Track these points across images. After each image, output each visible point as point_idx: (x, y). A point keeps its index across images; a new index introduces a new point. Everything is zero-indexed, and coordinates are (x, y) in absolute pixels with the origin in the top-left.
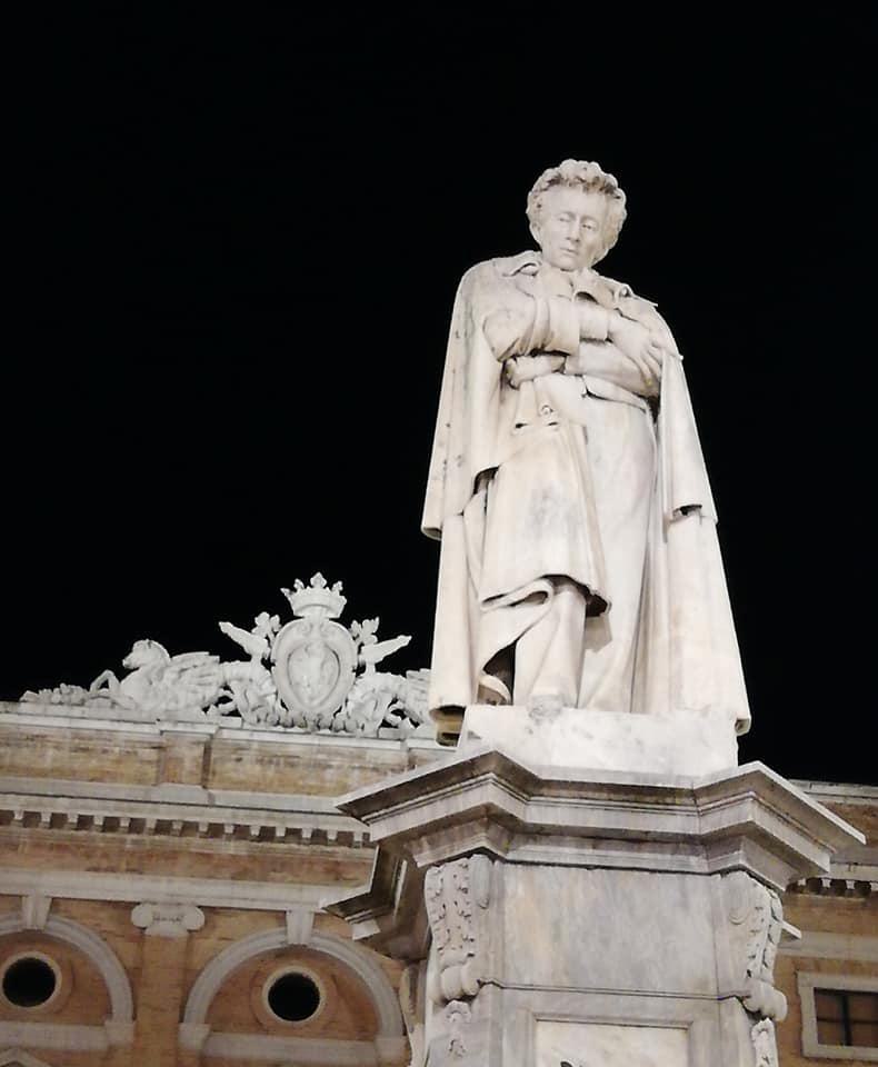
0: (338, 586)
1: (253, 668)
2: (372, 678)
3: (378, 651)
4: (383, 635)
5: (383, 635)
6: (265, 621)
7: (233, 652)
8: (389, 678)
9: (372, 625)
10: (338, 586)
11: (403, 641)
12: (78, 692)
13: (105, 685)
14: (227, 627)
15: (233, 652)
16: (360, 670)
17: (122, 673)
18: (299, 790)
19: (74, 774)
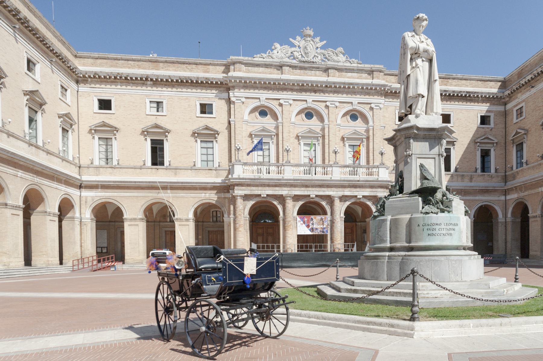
0: (312, 29)
1: (297, 49)
2: (319, 51)
3: (320, 45)
4: (321, 41)
6: (298, 38)
7: (292, 45)
9: (318, 38)
10: (312, 29)
12: (264, 55)
13: (269, 53)
14: (291, 39)
15: (292, 45)
17: (272, 50)
18: (308, 76)
19: (266, 73)
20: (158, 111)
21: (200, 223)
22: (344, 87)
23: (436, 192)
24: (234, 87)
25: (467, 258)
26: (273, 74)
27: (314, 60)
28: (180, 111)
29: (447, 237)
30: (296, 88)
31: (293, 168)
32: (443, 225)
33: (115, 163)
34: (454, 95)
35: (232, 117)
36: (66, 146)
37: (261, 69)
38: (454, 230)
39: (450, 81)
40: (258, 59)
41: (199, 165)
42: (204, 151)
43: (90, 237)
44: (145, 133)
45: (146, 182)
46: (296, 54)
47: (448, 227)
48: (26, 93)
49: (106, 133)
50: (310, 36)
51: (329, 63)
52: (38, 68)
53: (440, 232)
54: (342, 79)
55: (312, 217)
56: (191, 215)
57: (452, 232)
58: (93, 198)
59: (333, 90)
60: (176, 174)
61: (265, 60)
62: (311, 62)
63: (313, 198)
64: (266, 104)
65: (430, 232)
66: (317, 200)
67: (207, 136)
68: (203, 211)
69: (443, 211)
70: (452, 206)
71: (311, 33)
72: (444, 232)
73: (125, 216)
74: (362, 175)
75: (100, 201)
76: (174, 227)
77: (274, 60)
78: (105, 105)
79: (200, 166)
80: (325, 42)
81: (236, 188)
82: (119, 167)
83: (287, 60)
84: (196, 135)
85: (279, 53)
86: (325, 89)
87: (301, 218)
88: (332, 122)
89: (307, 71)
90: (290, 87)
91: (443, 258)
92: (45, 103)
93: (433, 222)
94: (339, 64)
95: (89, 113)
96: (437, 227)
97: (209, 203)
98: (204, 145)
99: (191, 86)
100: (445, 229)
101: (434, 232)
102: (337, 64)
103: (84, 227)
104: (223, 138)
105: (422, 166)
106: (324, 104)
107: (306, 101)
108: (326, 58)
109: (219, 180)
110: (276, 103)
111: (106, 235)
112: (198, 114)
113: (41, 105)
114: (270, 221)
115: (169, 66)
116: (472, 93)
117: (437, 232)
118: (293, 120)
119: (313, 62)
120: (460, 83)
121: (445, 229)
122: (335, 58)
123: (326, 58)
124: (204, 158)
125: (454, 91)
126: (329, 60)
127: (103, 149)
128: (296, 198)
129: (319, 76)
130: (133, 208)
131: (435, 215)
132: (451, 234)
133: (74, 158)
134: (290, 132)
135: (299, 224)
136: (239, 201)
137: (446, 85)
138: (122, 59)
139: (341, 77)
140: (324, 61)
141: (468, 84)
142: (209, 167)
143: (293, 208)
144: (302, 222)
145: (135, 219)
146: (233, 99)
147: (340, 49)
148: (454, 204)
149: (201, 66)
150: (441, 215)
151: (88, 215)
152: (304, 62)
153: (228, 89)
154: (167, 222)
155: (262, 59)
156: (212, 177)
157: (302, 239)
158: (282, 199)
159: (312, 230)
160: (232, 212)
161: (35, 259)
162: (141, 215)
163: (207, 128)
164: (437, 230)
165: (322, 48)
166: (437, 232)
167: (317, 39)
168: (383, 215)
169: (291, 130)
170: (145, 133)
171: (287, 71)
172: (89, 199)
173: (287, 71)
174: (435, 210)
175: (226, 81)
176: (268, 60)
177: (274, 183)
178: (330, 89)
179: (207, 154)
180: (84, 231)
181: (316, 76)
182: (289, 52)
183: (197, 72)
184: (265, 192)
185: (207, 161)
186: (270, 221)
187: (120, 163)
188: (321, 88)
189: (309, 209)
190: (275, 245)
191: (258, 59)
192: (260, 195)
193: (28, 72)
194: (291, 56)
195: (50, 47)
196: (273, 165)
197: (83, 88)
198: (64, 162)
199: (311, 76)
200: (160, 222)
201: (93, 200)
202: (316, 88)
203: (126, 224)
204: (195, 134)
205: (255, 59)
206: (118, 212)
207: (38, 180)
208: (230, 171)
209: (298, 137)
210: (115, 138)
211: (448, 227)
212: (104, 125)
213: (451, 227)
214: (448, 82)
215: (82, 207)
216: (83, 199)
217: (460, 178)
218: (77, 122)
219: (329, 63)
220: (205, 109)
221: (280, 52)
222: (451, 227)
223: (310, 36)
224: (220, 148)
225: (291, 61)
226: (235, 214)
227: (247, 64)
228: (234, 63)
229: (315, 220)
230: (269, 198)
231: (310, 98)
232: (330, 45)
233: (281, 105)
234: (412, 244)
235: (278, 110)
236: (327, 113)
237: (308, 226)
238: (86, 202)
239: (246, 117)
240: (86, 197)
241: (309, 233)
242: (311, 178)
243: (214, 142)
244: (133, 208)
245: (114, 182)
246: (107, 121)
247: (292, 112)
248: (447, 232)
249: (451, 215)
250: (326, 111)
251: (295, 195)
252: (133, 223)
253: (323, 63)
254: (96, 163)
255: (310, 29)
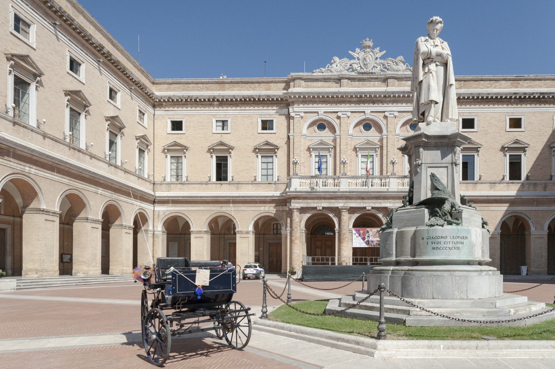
0: (371, 40)
1: (356, 61)
2: (378, 61)
3: (379, 55)
4: (381, 51)
5: (380, 51)
6: (358, 50)
7: (351, 58)
8: (382, 61)
9: (378, 49)
10: (371, 40)
11: (385, 52)
12: (323, 70)
13: (328, 67)
14: (350, 52)
15: (351, 58)
16: (377, 58)
17: (331, 64)
18: (366, 87)
19: (324, 87)
20: (223, 129)
21: (261, 236)
22: (404, 96)
23: (444, 203)
24: (293, 103)
25: (476, 274)
26: (332, 87)
27: (373, 71)
28: (244, 128)
29: (454, 251)
30: (354, 100)
31: (349, 180)
32: (449, 237)
33: (184, 179)
34: (525, 97)
35: (291, 131)
36: (142, 165)
37: (320, 84)
38: (462, 243)
39: (521, 82)
40: (317, 74)
41: (259, 179)
42: (265, 166)
43: (161, 248)
44: (211, 150)
45: (211, 197)
46: (355, 66)
47: (455, 241)
48: (108, 119)
49: (176, 152)
50: (369, 47)
51: (389, 72)
52: (119, 96)
53: (445, 246)
54: (402, 88)
55: (368, 229)
56: (251, 228)
57: (460, 246)
58: (164, 212)
59: (392, 99)
60: (238, 188)
61: (324, 74)
62: (370, 73)
63: (369, 210)
64: (324, 118)
65: (435, 246)
66: (373, 212)
67: (267, 151)
68: (264, 224)
69: (450, 223)
70: (461, 218)
71: (371, 44)
72: (451, 245)
73: (192, 229)
74: (376, 186)
75: (170, 215)
76: (235, 240)
77: (333, 74)
78: (177, 126)
79: (260, 180)
80: (385, 52)
81: (293, 201)
82: (188, 183)
83: (345, 72)
84: (257, 150)
85: (338, 66)
86: (384, 99)
87: (356, 231)
88: (391, 132)
89: (366, 82)
90: (348, 99)
91: (446, 274)
92: (124, 127)
93: (437, 235)
94: (399, 73)
95: (163, 134)
96: (442, 240)
97: (269, 216)
98: (265, 160)
99: (253, 104)
100: (451, 243)
101: (439, 246)
102: (396, 73)
103: (156, 239)
104: (282, 153)
105: (433, 176)
106: (383, 114)
107: (364, 112)
108: (386, 68)
109: (278, 194)
110: (334, 115)
111: (177, 246)
112: (260, 130)
113: (120, 129)
114: (328, 234)
115: (234, 87)
116: (547, 93)
117: (442, 245)
118: (351, 132)
119: (372, 73)
120: (533, 84)
121: (451, 243)
122: (395, 67)
123: (386, 68)
124: (265, 172)
125: (525, 94)
126: (388, 70)
127: (174, 167)
128: (352, 210)
129: (377, 87)
130: (199, 221)
131: (440, 227)
132: (458, 248)
133: (149, 176)
134: (347, 144)
135: (354, 237)
136: (296, 214)
137: (516, 87)
138: (193, 83)
139: (400, 86)
140: (384, 71)
141: (542, 85)
142: (269, 181)
143: (348, 220)
144: (357, 235)
145: (200, 232)
146: (292, 114)
147: (401, 58)
148: (464, 215)
149: (263, 84)
150: (447, 227)
151: (160, 227)
152: (362, 73)
153: (288, 105)
154: (231, 234)
155: (321, 74)
156: (271, 191)
157: (356, 251)
158: (337, 211)
159: (368, 243)
160: (289, 225)
161: (113, 268)
162: (206, 228)
163: (268, 144)
164: (442, 243)
165: (382, 58)
166: (442, 245)
167: (377, 50)
168: (391, 228)
169: (349, 142)
170: (211, 150)
171: (345, 83)
172: (161, 213)
173: (345, 83)
174: (441, 221)
175: (286, 97)
176: (327, 74)
177: (330, 196)
178: (388, 99)
179: (267, 169)
180: (156, 243)
181: (374, 86)
182: (348, 65)
183: (260, 90)
184: (321, 205)
185: (267, 175)
186: (328, 234)
187: (189, 179)
188: (380, 99)
189: (365, 221)
190: (330, 258)
191: (317, 74)
192: (316, 208)
193: (110, 100)
194: (349, 69)
195: (130, 76)
196: (331, 178)
197: (159, 112)
198: (140, 179)
199: (370, 87)
200: (224, 234)
201: (164, 214)
202: (375, 99)
203: (192, 236)
204: (257, 150)
205: (314, 74)
206: (187, 226)
207: (115, 196)
208: (288, 185)
209: (355, 149)
210: (185, 156)
211: (455, 241)
212: (176, 144)
213: (458, 240)
214: (519, 83)
215: (155, 220)
216: (156, 213)
217: (531, 187)
218: (152, 143)
219: (389, 72)
220: (267, 125)
221: (339, 65)
222: (458, 240)
223: (369, 47)
224: (279, 163)
225: (349, 73)
226: (291, 227)
227: (307, 80)
228: (294, 80)
229: (370, 233)
230: (324, 210)
231: (368, 109)
232: (391, 54)
233: (339, 118)
234: (417, 258)
235: (336, 123)
236: (385, 123)
237: (364, 239)
238: (158, 216)
239: (305, 131)
240: (159, 211)
241: (364, 245)
242: (367, 190)
243: (274, 157)
244: (199, 221)
245: (183, 197)
246: (178, 141)
247: (350, 124)
248: (454, 245)
249: (459, 227)
250: (385, 121)
251: (351, 208)
252: (198, 235)
253: (382, 73)
254: (168, 179)
255: (370, 40)
